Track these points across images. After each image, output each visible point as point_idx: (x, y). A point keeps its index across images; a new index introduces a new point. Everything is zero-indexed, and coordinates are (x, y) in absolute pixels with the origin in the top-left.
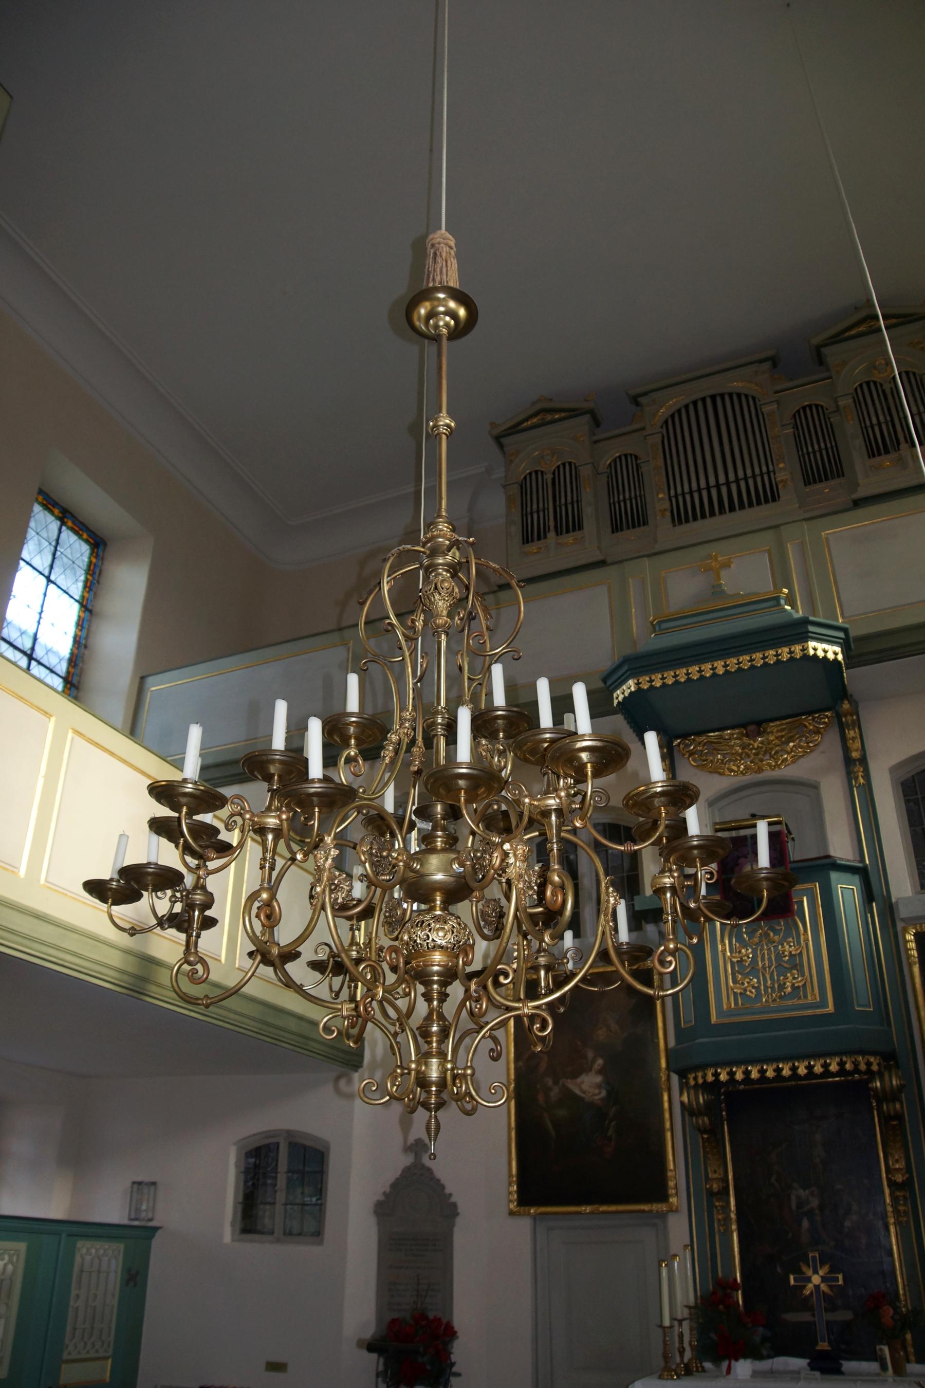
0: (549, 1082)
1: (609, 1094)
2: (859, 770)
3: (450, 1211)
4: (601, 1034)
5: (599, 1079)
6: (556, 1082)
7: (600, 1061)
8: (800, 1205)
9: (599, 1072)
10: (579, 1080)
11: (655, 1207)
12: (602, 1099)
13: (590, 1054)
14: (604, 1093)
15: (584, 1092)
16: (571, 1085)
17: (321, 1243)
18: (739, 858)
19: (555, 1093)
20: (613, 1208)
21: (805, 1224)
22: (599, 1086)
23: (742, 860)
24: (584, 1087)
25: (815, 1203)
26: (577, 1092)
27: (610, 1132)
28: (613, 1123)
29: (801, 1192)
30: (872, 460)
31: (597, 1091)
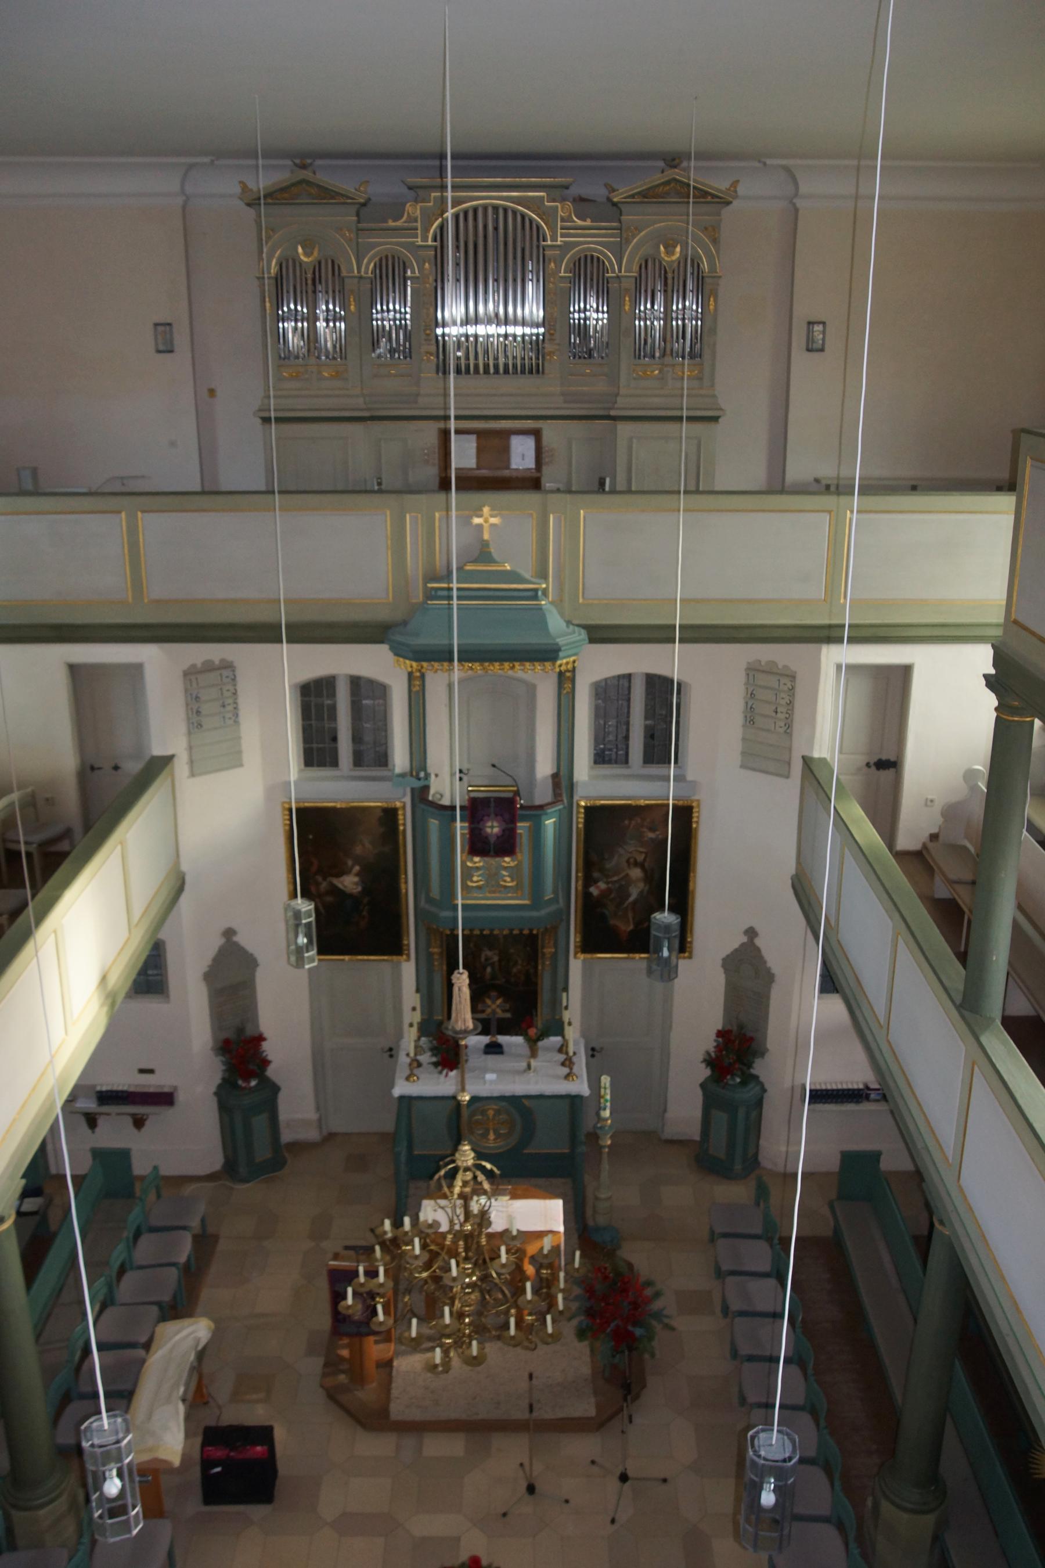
0: (319, 878)
1: (364, 889)
2: (568, 685)
3: (250, 962)
4: (358, 850)
5: (356, 879)
6: (325, 879)
7: (357, 868)
8: (486, 960)
9: (357, 875)
10: (342, 879)
11: (395, 958)
12: (359, 892)
13: (350, 863)
14: (359, 889)
15: (345, 887)
16: (336, 882)
17: (168, 1002)
18: (483, 816)
19: (324, 886)
20: (366, 957)
21: (489, 970)
22: (356, 884)
23: (486, 818)
24: (346, 884)
25: (496, 959)
26: (340, 886)
27: (365, 913)
28: (366, 908)
29: (489, 953)
30: (638, 361)
31: (355, 887)
